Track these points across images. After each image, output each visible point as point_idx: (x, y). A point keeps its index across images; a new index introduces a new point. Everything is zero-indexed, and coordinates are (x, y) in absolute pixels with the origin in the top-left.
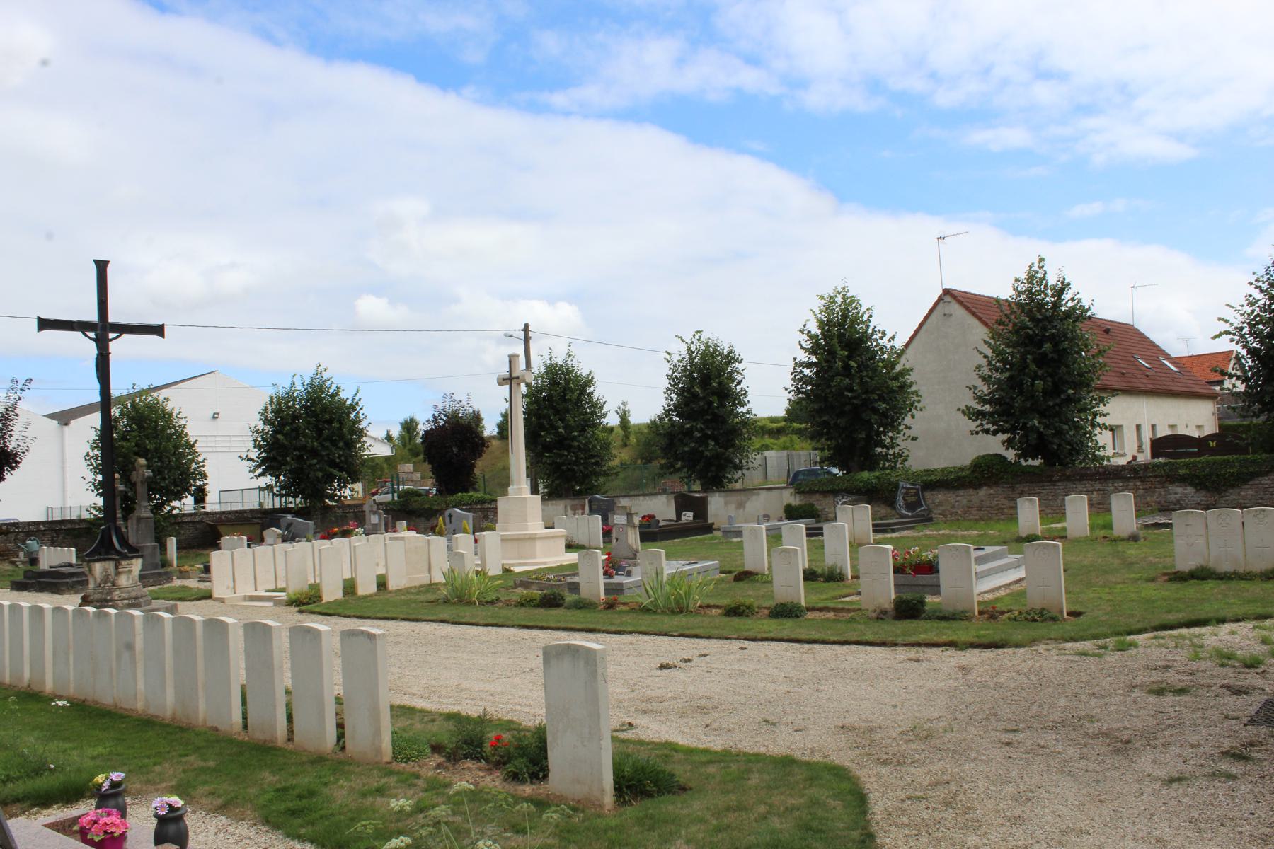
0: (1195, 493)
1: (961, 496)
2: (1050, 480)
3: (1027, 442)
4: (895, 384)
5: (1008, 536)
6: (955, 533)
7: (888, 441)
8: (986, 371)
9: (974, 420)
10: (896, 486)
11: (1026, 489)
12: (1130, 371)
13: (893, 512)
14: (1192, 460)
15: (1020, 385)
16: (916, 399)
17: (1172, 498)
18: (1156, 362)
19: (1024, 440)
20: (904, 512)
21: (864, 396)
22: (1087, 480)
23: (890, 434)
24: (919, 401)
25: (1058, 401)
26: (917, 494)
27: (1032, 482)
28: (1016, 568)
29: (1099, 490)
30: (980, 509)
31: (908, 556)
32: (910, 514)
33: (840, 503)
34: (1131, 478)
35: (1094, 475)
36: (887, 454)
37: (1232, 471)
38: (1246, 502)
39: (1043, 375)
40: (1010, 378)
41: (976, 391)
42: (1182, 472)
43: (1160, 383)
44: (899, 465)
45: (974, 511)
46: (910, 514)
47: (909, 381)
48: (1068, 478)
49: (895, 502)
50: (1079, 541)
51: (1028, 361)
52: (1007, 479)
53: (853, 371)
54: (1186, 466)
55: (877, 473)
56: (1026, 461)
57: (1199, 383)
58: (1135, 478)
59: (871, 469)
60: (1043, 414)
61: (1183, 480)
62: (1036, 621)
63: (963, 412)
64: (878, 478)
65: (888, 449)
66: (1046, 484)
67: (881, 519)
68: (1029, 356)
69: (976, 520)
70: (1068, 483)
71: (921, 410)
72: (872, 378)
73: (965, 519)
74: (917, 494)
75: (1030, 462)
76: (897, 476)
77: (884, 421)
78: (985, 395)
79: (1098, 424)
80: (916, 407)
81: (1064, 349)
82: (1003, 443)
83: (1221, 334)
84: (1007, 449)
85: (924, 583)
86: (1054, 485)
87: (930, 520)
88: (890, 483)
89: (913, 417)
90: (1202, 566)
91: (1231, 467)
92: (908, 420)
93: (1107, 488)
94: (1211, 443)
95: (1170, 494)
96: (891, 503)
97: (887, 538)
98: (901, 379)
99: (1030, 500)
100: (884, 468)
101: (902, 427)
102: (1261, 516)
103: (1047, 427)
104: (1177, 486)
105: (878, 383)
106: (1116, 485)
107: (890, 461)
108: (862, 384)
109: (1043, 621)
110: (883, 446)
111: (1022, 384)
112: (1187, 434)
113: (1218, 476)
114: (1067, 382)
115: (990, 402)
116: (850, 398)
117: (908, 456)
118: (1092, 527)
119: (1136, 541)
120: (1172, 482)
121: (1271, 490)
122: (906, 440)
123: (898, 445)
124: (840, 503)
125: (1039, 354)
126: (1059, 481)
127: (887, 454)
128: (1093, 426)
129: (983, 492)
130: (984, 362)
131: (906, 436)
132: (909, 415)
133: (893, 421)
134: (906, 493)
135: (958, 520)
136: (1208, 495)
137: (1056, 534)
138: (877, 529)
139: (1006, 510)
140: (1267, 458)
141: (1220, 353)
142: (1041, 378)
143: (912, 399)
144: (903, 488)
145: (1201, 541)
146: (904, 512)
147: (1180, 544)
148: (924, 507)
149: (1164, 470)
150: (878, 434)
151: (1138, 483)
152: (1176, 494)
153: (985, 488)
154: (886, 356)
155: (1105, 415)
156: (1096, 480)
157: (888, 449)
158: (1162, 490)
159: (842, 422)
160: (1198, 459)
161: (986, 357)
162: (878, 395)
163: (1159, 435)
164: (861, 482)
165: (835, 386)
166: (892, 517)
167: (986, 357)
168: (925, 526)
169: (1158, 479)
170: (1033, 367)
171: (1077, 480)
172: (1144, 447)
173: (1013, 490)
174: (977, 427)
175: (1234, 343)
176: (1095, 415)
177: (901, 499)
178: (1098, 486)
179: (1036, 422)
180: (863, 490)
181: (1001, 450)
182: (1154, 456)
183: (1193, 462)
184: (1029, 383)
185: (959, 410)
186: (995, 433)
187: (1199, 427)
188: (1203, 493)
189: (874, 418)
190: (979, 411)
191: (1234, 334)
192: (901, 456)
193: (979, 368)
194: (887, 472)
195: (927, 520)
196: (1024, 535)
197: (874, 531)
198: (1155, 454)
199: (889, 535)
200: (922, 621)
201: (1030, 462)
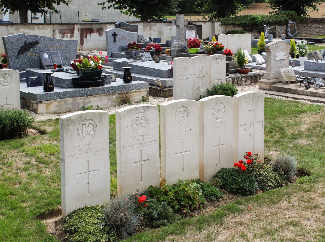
1: (282, 28)
20: (290, 34)
26: (294, 27)
46: (292, 35)
74: (294, 27)
86: (308, 25)
134: (291, 26)
144: (290, 23)
146: (290, 34)
148: (297, 33)
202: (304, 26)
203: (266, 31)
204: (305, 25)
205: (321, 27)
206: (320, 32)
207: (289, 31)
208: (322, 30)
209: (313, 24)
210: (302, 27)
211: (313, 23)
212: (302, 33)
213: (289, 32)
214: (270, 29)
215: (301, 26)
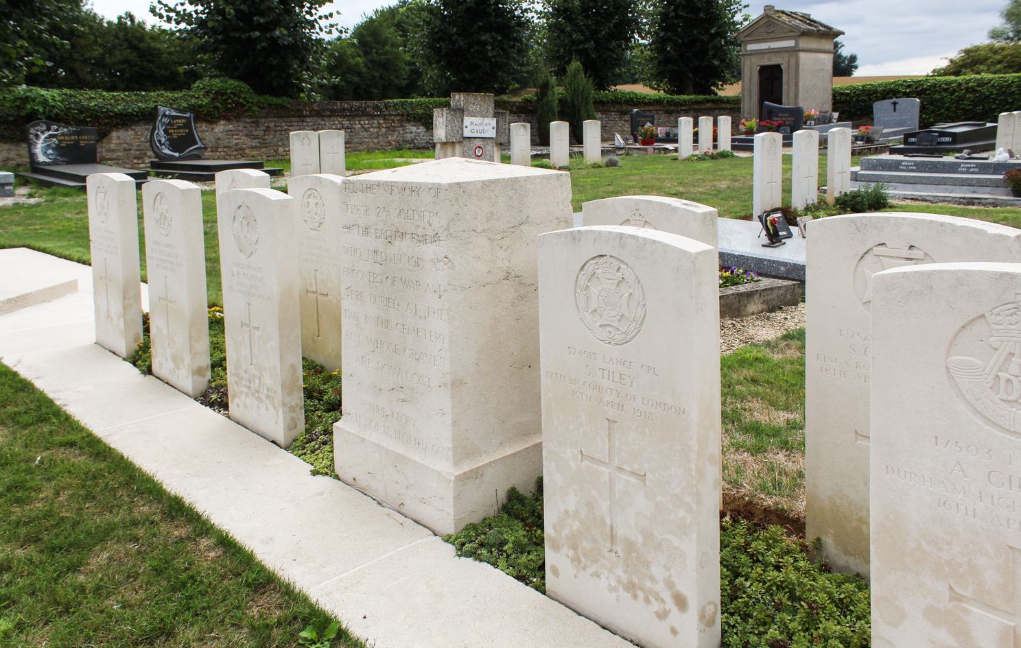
11: (272, 125)
17: (409, 137)
20: (167, 151)
22: (337, 116)
26: (187, 125)
29: (347, 128)
46: (177, 155)
66: (294, 119)
74: (187, 125)
86: (303, 121)
93: (356, 126)
95: (406, 133)
104: (413, 126)
106: (362, 122)
120: (409, 121)
126: (309, 117)
129: (221, 127)
134: (169, 124)
139: (247, 151)
144: (165, 115)
146: (167, 151)
148: (199, 144)
151: (381, 121)
152: (411, 133)
153: (222, 122)
158: (401, 129)
169: (398, 118)
173: (258, 126)
178: (346, 123)
202: (288, 124)
203: (41, 141)
204: (291, 122)
205: (359, 126)
206: (356, 140)
207: (163, 140)
208: (366, 134)
209: (323, 120)
210: (279, 128)
211: (324, 116)
212: (280, 146)
214: (63, 134)
215: (275, 126)
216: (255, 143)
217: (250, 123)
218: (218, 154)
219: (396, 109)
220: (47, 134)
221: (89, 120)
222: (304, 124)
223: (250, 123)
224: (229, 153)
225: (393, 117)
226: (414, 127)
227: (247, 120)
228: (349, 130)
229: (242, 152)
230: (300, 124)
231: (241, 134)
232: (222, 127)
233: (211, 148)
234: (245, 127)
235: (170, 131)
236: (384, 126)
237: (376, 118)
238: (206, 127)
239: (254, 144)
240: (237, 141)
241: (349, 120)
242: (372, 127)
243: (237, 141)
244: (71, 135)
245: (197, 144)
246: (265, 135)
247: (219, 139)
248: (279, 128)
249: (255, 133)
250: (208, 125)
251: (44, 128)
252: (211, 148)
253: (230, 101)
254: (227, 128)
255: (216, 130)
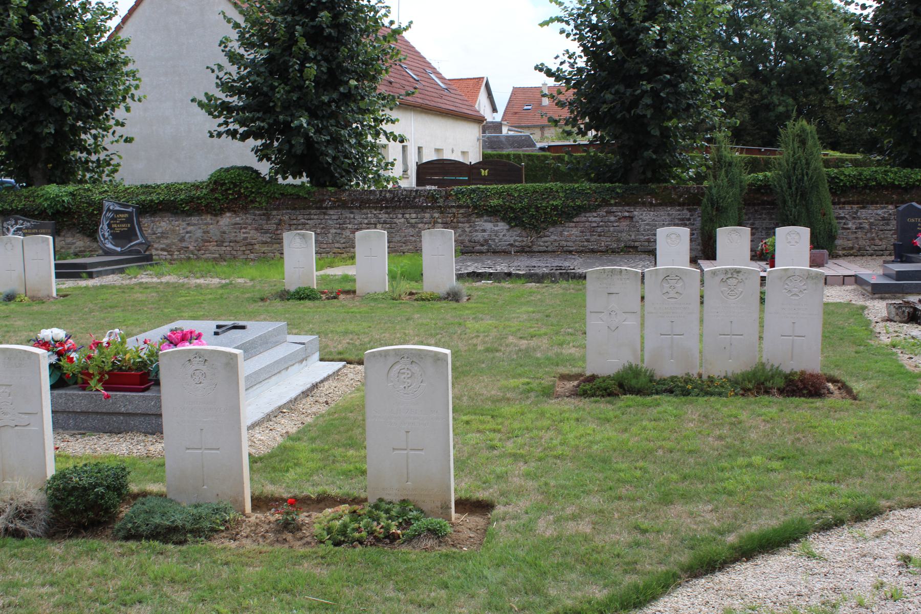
0: (508, 230)
1: (194, 225)
2: (320, 206)
3: (289, 151)
4: (101, 59)
5: (267, 290)
6: (186, 280)
7: (91, 141)
8: (235, 46)
9: (215, 117)
10: (100, 207)
11: (286, 218)
12: (398, 81)
13: (95, 245)
14: (506, 186)
15: (286, 67)
16: (134, 83)
17: (479, 236)
18: (423, 75)
19: (287, 147)
21: (52, 72)
22: (373, 208)
23: (93, 132)
24: (137, 87)
25: (335, 96)
27: (295, 209)
28: (301, 361)
30: (220, 243)
31: (95, 353)
32: (119, 249)
33: (12, 230)
34: (427, 207)
35: (379, 201)
36: (87, 162)
37: (555, 203)
38: (569, 244)
39: (316, 57)
40: (269, 60)
41: (221, 74)
42: (494, 202)
43: (429, 98)
44: (105, 178)
45: (212, 247)
46: (119, 249)
47: (123, 56)
48: (344, 205)
49: (96, 231)
50: (375, 300)
51: (297, 34)
52: (260, 203)
53: (36, 32)
54: (499, 194)
55: (71, 188)
56: (285, 178)
57: (465, 102)
58: (432, 208)
59: (63, 182)
60: (313, 114)
61: (493, 213)
62: (392, 538)
63: (201, 105)
64: (72, 194)
65: (89, 153)
66: (313, 211)
67: (76, 255)
68: (297, 27)
69: (214, 259)
70: (343, 212)
71: (140, 100)
72: (66, 46)
73: (198, 258)
74: (129, 220)
75: (290, 180)
76: (100, 193)
77: (84, 110)
78: (234, 81)
79: (385, 132)
80: (133, 95)
81: (346, 24)
82: (256, 150)
83: (552, 20)
84: (260, 160)
85: (130, 409)
86: (325, 214)
87: (149, 258)
88: (91, 203)
89: (128, 109)
90: (631, 367)
91: (554, 198)
92: (120, 113)
94: (483, 171)
95: (476, 231)
96: (92, 233)
97: (80, 288)
98: (111, 52)
99: (303, 236)
100: (81, 182)
101: (112, 122)
102: (733, 282)
103: (318, 131)
104: (486, 221)
105: (76, 54)
106: (407, 216)
107: (93, 171)
108: (50, 52)
109: (410, 540)
110: (83, 149)
111: (287, 70)
112: (453, 158)
113: (537, 209)
114: (348, 71)
115: (239, 92)
116: (31, 73)
117: (118, 165)
118: (393, 277)
119: (457, 301)
120: (480, 215)
121: (599, 230)
122: (117, 141)
123: (105, 149)
124: (12, 230)
125: (313, 27)
126: (331, 208)
127: (87, 162)
128: (377, 134)
129: (226, 220)
130: (234, 35)
131: (117, 135)
132: (122, 105)
133: (99, 113)
134: (113, 219)
135: (189, 258)
136: (524, 233)
137: (337, 287)
138: (63, 271)
139: (257, 247)
140: (597, 188)
141: (471, 79)
142: (314, 60)
143: (127, 83)
144: (109, 210)
145: (632, 322)
146: (109, 246)
147: (595, 325)
148: (141, 240)
149: (472, 199)
150: (75, 131)
151: (436, 215)
152: (484, 231)
153: (228, 214)
154: (89, 16)
155: (393, 122)
156: (381, 208)
157: (89, 153)
158: (467, 225)
159: (17, 108)
160: (514, 186)
161: (236, 26)
162: (75, 71)
163: (425, 160)
164: (46, 200)
165: (6, 52)
166: (92, 253)
167: (236, 26)
168: (140, 267)
169: (462, 211)
170: (303, 43)
171: (357, 208)
172: (409, 172)
173: (268, 219)
174: (220, 125)
175: (564, 35)
176: (378, 121)
177: (106, 227)
178: (383, 216)
179: (304, 121)
180: (49, 212)
181: (252, 161)
182: (419, 182)
183: (508, 191)
184: (297, 67)
185: (193, 100)
186: (244, 137)
187: (463, 153)
188: (518, 231)
189: (68, 105)
190: (224, 102)
191: (568, 23)
192: (109, 164)
193: (223, 43)
194: (87, 186)
195: (144, 258)
196: (293, 289)
197: (58, 276)
198: (420, 181)
199: (83, 283)
200: (114, 548)
201: (290, 180)
204: (310, 214)
207: (107, 234)
209: (352, 213)
210: (295, 222)
211: (352, 208)
213: (105, 239)
216: (266, 238)
217: (260, 215)
218: (224, 248)
219: (459, 199)
220: (15, 227)
221: (95, 212)
222: (326, 217)
223: (260, 215)
224: (235, 249)
225: (454, 210)
226: (487, 224)
227: (257, 212)
228: (388, 225)
229: (250, 247)
230: (322, 217)
231: (250, 227)
232: (228, 220)
233: (216, 242)
234: (254, 219)
235: (113, 226)
236: (440, 221)
237: (428, 211)
238: (211, 219)
239: (264, 239)
240: (245, 235)
241: (389, 214)
242: (422, 223)
243: (245, 235)
244: (32, 228)
245: (138, 239)
246: (277, 230)
247: (224, 233)
248: (295, 222)
249: (266, 227)
250: (213, 218)
251: (13, 222)
252: (216, 242)
253: (231, 192)
254: (233, 221)
255: (221, 223)
